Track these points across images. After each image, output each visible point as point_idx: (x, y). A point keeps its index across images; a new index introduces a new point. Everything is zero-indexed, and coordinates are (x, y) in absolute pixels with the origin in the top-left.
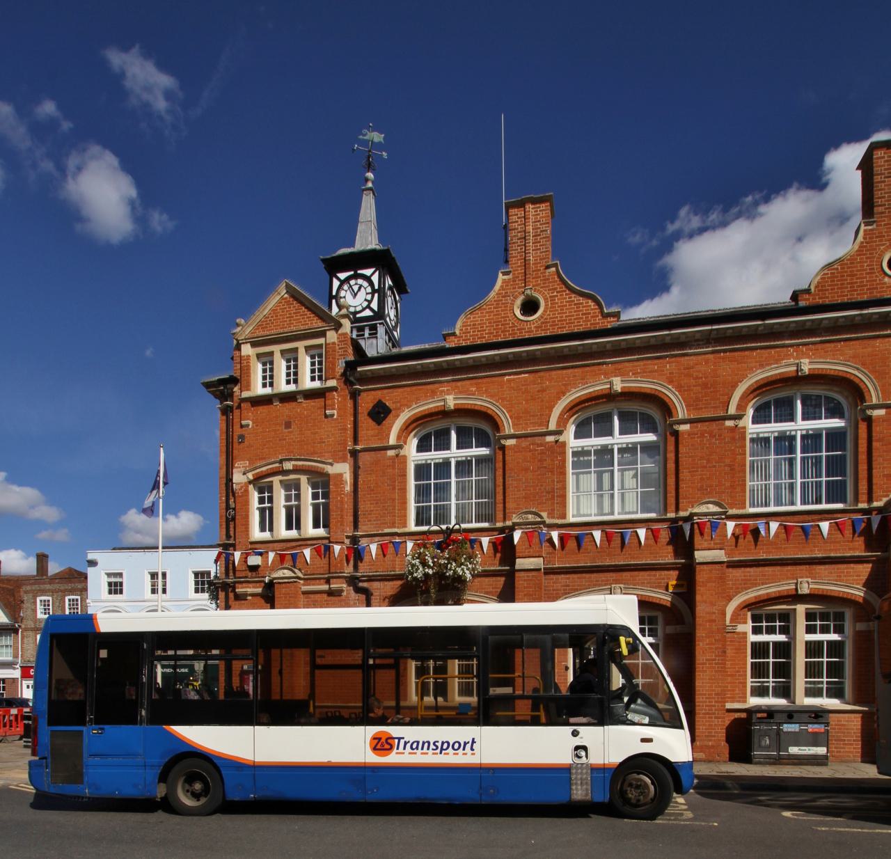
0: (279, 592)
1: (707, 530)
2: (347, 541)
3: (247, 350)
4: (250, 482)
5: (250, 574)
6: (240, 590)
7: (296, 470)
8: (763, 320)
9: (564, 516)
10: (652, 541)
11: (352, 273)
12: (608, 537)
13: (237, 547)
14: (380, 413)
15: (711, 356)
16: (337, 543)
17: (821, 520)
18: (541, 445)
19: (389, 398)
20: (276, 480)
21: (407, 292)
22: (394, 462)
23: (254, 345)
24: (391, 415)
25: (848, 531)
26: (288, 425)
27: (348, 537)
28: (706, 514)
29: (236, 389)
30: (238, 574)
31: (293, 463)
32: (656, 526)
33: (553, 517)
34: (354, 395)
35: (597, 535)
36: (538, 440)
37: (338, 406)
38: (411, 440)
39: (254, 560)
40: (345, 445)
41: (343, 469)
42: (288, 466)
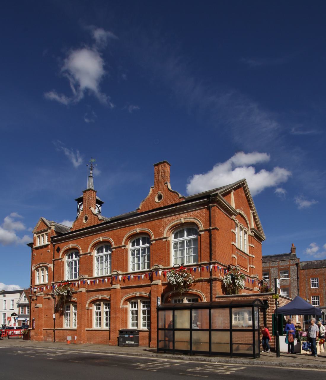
0: (39, 298)
1: (115, 279)
2: (52, 285)
3: (35, 235)
4: (35, 270)
5: (34, 294)
6: (32, 298)
7: (43, 266)
8: (127, 219)
9: (92, 276)
10: (108, 282)
11: (82, 203)
12: (100, 281)
13: (32, 287)
14: (58, 250)
15: (119, 229)
16: (49, 285)
17: (142, 274)
18: (87, 257)
19: (60, 245)
20: (40, 269)
21: (103, 203)
22: (61, 263)
23: (37, 234)
24: (60, 250)
25: (148, 278)
26: (42, 254)
27: (52, 283)
28: (114, 275)
29: (33, 245)
30: (32, 294)
31: (42, 264)
32: (109, 278)
33: (89, 276)
34: (54, 245)
35: (97, 281)
36: (86, 255)
37: (50, 249)
38: (65, 257)
39: (35, 290)
40: (51, 259)
41: (51, 266)
42: (41, 265)
